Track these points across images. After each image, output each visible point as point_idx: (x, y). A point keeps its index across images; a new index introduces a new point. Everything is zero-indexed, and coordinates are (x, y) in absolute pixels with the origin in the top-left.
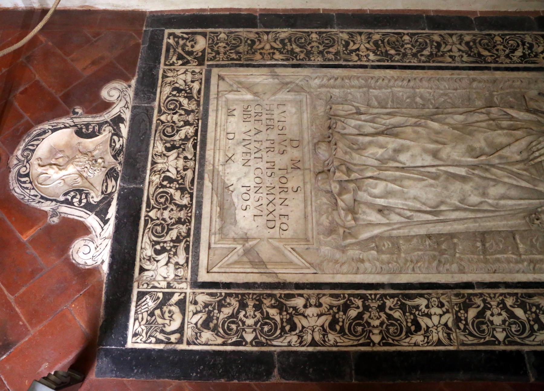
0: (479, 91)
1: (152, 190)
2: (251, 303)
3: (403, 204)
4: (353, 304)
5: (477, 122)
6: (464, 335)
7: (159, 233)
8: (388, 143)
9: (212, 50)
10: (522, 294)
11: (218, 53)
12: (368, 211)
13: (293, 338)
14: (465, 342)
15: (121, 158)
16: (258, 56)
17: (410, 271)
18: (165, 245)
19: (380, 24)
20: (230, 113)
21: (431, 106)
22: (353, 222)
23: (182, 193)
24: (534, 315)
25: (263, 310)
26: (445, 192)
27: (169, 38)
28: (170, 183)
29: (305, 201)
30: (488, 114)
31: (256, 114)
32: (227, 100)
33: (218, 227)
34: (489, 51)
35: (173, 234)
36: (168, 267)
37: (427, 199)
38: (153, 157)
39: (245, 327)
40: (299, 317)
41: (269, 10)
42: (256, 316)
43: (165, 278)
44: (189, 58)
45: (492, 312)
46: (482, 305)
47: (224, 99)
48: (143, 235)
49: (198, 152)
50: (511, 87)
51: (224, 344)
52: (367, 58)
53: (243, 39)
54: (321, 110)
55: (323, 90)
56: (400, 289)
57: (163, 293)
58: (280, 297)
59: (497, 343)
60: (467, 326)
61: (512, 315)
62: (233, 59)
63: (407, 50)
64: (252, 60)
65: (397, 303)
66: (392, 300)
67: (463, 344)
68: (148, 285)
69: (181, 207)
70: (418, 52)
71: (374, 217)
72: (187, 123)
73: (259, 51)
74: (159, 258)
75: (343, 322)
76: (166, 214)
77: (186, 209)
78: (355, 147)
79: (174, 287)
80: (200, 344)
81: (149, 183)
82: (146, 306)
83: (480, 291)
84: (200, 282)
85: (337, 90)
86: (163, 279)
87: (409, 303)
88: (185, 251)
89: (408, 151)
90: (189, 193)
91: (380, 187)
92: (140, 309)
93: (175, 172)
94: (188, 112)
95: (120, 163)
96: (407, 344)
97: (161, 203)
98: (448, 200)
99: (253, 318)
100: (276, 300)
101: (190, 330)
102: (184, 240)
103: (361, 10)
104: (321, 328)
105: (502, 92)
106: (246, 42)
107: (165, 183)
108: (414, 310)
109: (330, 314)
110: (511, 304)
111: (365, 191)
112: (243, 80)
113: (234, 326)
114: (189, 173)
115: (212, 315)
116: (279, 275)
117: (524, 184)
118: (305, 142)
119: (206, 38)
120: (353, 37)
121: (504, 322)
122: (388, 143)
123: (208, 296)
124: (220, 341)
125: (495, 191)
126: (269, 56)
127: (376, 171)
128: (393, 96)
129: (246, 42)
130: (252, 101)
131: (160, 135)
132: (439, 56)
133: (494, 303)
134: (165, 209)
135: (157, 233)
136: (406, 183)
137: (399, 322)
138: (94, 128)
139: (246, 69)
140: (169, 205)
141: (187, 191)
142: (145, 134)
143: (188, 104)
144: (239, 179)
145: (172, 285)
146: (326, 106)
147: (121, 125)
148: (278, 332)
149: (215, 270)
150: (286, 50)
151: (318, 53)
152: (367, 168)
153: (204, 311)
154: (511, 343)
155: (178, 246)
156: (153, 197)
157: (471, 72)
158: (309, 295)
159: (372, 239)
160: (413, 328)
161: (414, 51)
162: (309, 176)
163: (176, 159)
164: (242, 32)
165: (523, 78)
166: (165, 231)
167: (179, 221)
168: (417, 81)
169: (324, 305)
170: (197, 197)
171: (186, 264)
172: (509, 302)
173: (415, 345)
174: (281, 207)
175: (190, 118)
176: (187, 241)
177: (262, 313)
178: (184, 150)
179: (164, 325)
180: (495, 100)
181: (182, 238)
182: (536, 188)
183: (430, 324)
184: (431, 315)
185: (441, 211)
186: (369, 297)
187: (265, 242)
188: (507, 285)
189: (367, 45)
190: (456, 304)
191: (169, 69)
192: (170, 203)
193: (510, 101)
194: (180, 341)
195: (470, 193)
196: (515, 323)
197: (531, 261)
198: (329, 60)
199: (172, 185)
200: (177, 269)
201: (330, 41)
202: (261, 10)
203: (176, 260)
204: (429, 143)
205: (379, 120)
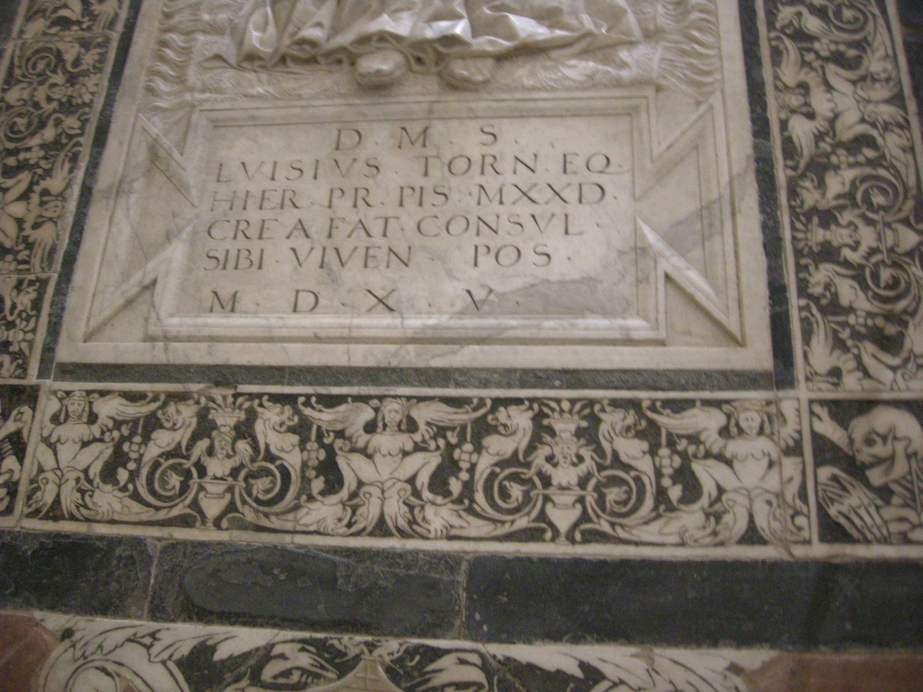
2: (819, 235)
4: (791, 23)
7: (629, 492)
16: (46, 234)
18: (667, 471)
23: (492, 430)
25: (835, 208)
31: (240, 235)
35: (632, 449)
36: (735, 456)
40: (839, 125)
42: (850, 224)
43: (771, 465)
48: (637, 544)
62: (37, 305)
64: (53, 250)
69: (542, 430)
72: (244, 430)
74: (708, 487)
76: (565, 475)
77: (547, 416)
79: (796, 436)
81: (450, 538)
84: (776, 365)
86: (775, 470)
88: (684, 409)
93: (417, 459)
95: (371, 646)
97: (526, 494)
100: (803, 176)
102: (650, 414)
104: (859, 86)
107: (455, 486)
109: (823, 68)
113: (886, 274)
114: (423, 414)
115: (863, 330)
123: (814, 342)
131: (277, 514)
134: (546, 481)
135: (629, 499)
140: (533, 470)
142: (265, 568)
143: (173, 429)
145: (791, 443)
147: (221, 654)
148: (882, 172)
153: (855, 351)
155: (669, 434)
156: (503, 523)
158: (782, 107)
166: (621, 474)
170: (509, 386)
171: (726, 407)
175: (226, 419)
176: (653, 408)
177: (842, 208)
178: (340, 434)
181: (644, 423)
192: (528, 465)
200: (741, 431)
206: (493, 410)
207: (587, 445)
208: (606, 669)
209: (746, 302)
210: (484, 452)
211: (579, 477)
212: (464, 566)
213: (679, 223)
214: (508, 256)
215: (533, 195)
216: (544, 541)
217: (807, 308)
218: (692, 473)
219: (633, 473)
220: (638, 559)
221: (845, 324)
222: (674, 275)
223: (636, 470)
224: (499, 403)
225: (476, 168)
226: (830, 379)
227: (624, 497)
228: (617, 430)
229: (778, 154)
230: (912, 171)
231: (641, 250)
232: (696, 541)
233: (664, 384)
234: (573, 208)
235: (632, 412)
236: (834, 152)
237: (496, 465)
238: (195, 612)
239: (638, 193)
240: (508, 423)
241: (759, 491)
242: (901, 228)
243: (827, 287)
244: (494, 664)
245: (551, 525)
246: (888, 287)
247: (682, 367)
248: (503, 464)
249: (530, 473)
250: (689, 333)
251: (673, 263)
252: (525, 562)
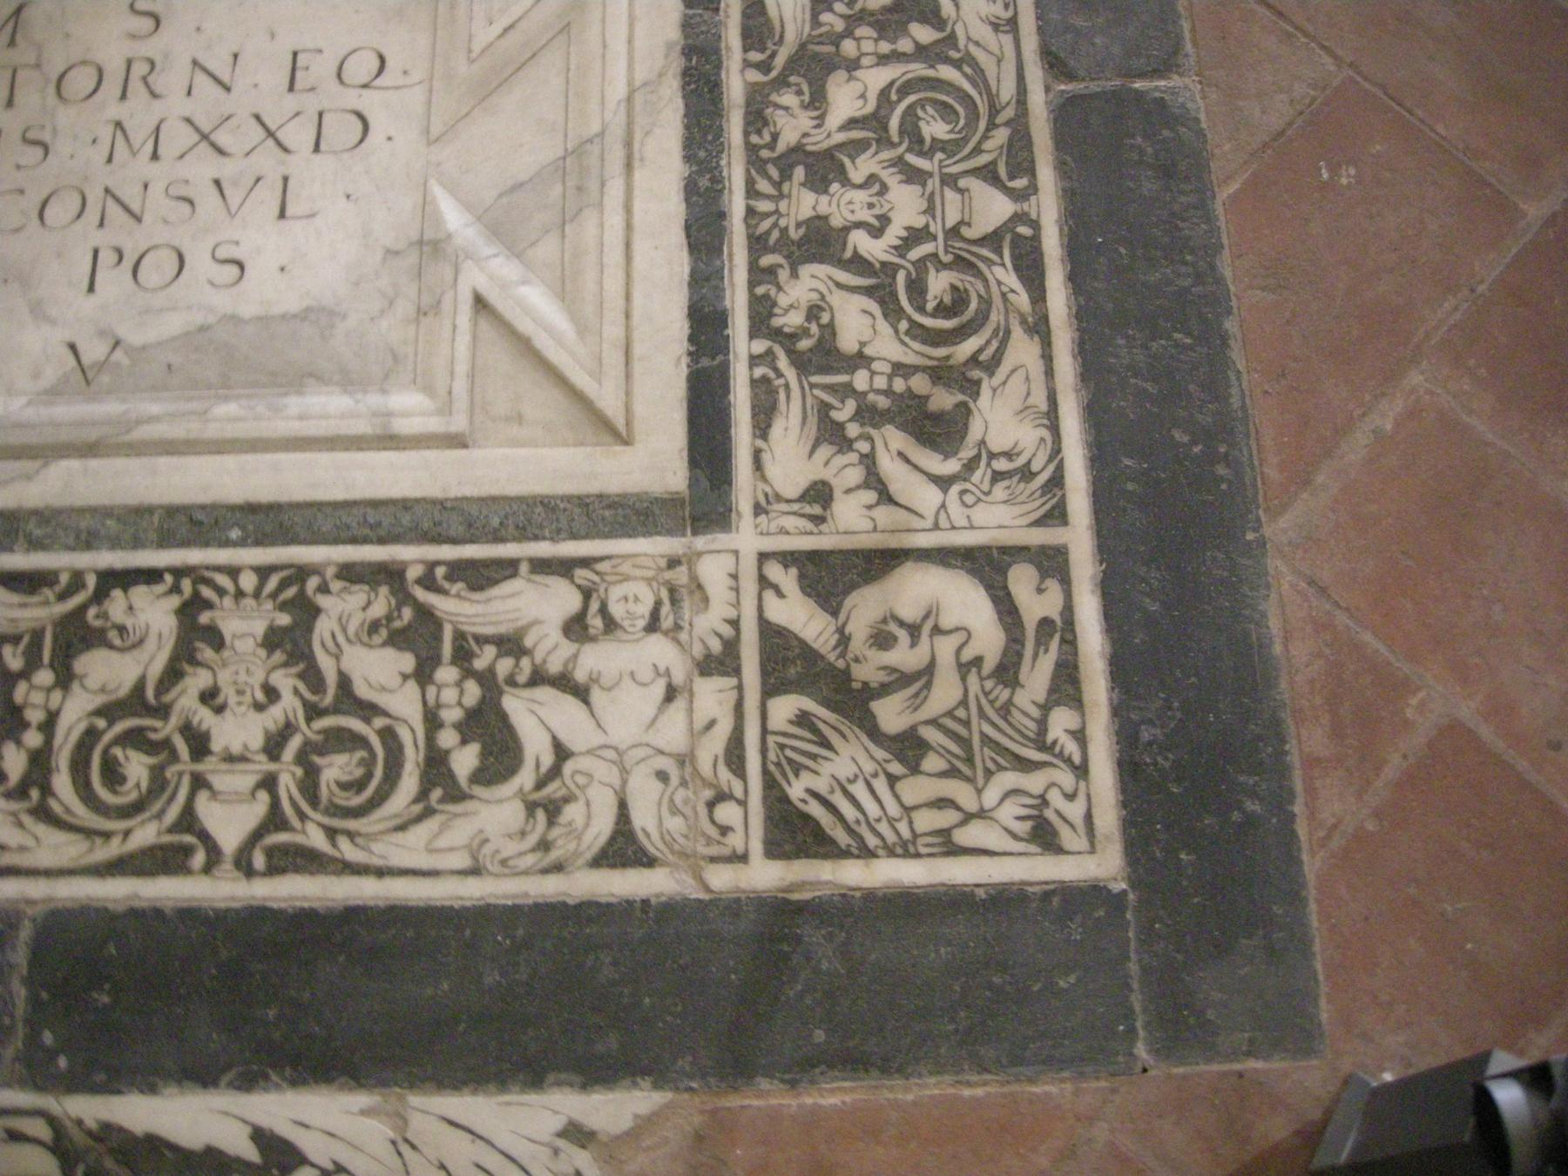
2: (804, 204)
7: (369, 764)
18: (451, 715)
25: (840, 146)
35: (379, 671)
36: (594, 679)
39: (935, 227)
42: (872, 179)
43: (671, 694)
48: (381, 872)
51: (1040, 328)
57: (770, 690)
58: (764, 67)
68: (722, 797)
69: (196, 635)
74: (535, 746)
76: (238, 730)
77: (209, 605)
79: (727, 631)
80: (1057, 450)
82: (859, 790)
84: (693, 482)
86: (680, 703)
88: (494, 582)
92: (883, 828)
97: (157, 774)
99: (884, 190)
100: (781, 82)
101: (981, 515)
102: (421, 594)
113: (938, 284)
115: (883, 402)
123: (776, 431)
124: (1023, 350)
134: (199, 744)
135: (369, 776)
140: (174, 721)
141: (83, 608)
148: (946, 72)
155: (460, 636)
156: (107, 835)
166: (355, 724)
170: (137, 544)
171: (581, 574)
176: (428, 582)
181: (407, 613)
192: (163, 711)
194: (1052, 563)
200: (611, 625)
203: (554, 635)
206: (100, 595)
207: (286, 665)
208: (309, 1143)
209: (638, 350)
210: (75, 686)
211: (267, 734)
212: (25, 933)
213: (517, 187)
214: (157, 268)
215: (222, 138)
216: (188, 871)
217: (767, 358)
218: (504, 717)
219: (379, 722)
220: (381, 904)
221: (847, 390)
222: (493, 297)
223: (386, 714)
224: (114, 580)
225: (111, 87)
226: (808, 510)
227: (359, 772)
228: (351, 630)
229: (732, 37)
230: (1009, 67)
231: (431, 247)
232: (504, 862)
233: (457, 529)
234: (302, 164)
235: (384, 590)
236: (848, 33)
237: (98, 712)
239: (436, 129)
240: (129, 623)
241: (641, 753)
242: (975, 185)
243: (813, 312)
244: (79, 1138)
245: (205, 837)
246: (942, 310)
247: (495, 491)
248: (110, 711)
249: (167, 729)
250: (520, 419)
251: (492, 271)
252: (148, 918)
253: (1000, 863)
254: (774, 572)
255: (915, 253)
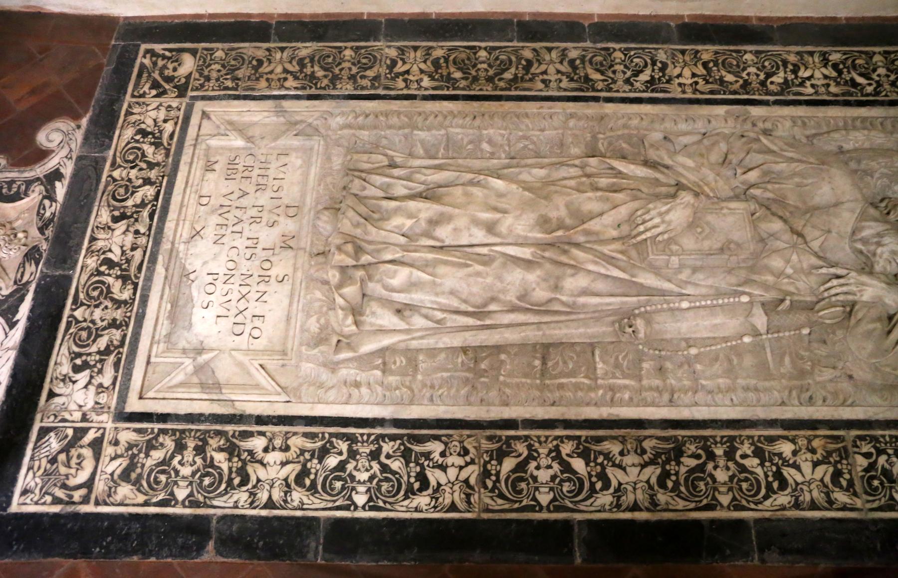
0: (577, 132)
1: (84, 277)
2: (191, 444)
3: (432, 302)
4: (335, 447)
5: (565, 179)
6: (491, 498)
7: (84, 341)
8: (420, 211)
9: (201, 75)
10: (587, 437)
11: (208, 79)
12: (379, 311)
13: (242, 496)
14: (490, 507)
15: (49, 232)
17: (426, 402)
18: (89, 359)
19: (447, 35)
20: (209, 168)
21: (503, 156)
22: (354, 328)
23: (124, 283)
24: (599, 468)
26: (499, 284)
27: (144, 57)
28: (110, 268)
29: (292, 296)
30: (582, 167)
32: (209, 148)
33: (164, 333)
34: (602, 73)
35: (102, 343)
37: (471, 294)
38: (93, 231)
39: (178, 478)
41: (291, 15)
42: (195, 463)
43: (80, 406)
44: (167, 87)
45: (539, 464)
46: (526, 453)
47: (204, 146)
48: (61, 345)
49: (155, 224)
50: (625, 126)
51: (146, 504)
52: (419, 84)
53: (246, 57)
54: (337, 162)
55: (346, 132)
56: (407, 428)
59: (537, 508)
60: (498, 484)
61: (567, 467)
63: (480, 73)
65: (399, 449)
66: (392, 443)
67: (487, 510)
68: (56, 416)
69: (118, 303)
70: (496, 75)
71: (387, 319)
73: (265, 76)
74: (77, 377)
75: (316, 474)
76: (98, 313)
78: (376, 216)
80: (113, 505)
82: (48, 448)
83: (526, 433)
85: (367, 133)
87: (417, 448)
89: (448, 223)
90: (133, 283)
91: (402, 275)
94: (151, 166)
95: (46, 239)
96: (404, 509)
97: (93, 298)
98: (501, 296)
99: (192, 465)
100: (227, 440)
101: (102, 483)
103: (423, 14)
104: (284, 483)
105: (612, 134)
106: (250, 62)
108: (423, 459)
109: (299, 462)
110: (568, 452)
111: (378, 281)
112: (235, 118)
113: (163, 478)
114: (138, 254)
115: (136, 461)
116: (237, 404)
117: (616, 273)
118: (306, 209)
119: (195, 57)
120: (403, 54)
121: (553, 478)
122: (420, 211)
123: (134, 434)
124: (141, 498)
125: (573, 283)
126: (278, 84)
127: (398, 252)
128: (448, 140)
129: (250, 62)
130: (244, 149)
132: (526, 81)
133: (543, 451)
134: (97, 306)
136: (441, 270)
137: (397, 476)
138: (19, 187)
139: (242, 102)
144: (205, 263)
146: (346, 156)
149: (151, 394)
150: (303, 75)
151: (349, 78)
152: (387, 248)
153: (125, 455)
154: (558, 509)
155: (105, 360)
157: (571, 104)
158: (274, 434)
159: (382, 352)
160: (417, 486)
161: (491, 72)
162: (303, 258)
163: (124, 233)
164: (249, 49)
165: (646, 115)
166: (92, 338)
167: (114, 324)
168: (486, 117)
169: (293, 449)
171: (111, 387)
172: (566, 448)
173: (417, 510)
174: (257, 303)
175: (153, 174)
176: (119, 353)
177: (204, 459)
179: (67, 476)
180: (600, 145)
182: (634, 279)
183: (443, 481)
184: (447, 466)
185: (490, 312)
186: (360, 439)
187: (226, 355)
188: (568, 424)
189: (423, 66)
190: (487, 452)
191: (137, 103)
192: (105, 298)
193: (622, 148)
195: (534, 285)
196: (569, 480)
197: (612, 389)
198: (363, 88)
199: (111, 272)
201: (370, 61)
202: (280, 15)
204: (482, 211)
205: (418, 176)
217: (152, 432)
221: (140, 451)
224: (136, 285)
238: (75, 175)
243: (162, 445)
253: (25, 479)
254: (101, 431)
255: (172, 473)
